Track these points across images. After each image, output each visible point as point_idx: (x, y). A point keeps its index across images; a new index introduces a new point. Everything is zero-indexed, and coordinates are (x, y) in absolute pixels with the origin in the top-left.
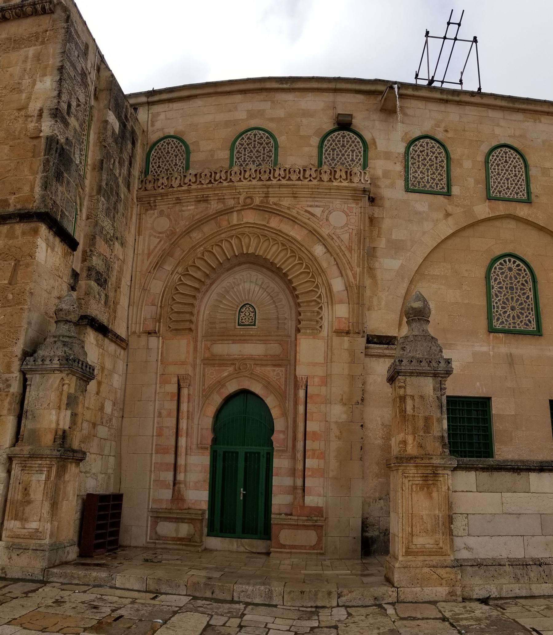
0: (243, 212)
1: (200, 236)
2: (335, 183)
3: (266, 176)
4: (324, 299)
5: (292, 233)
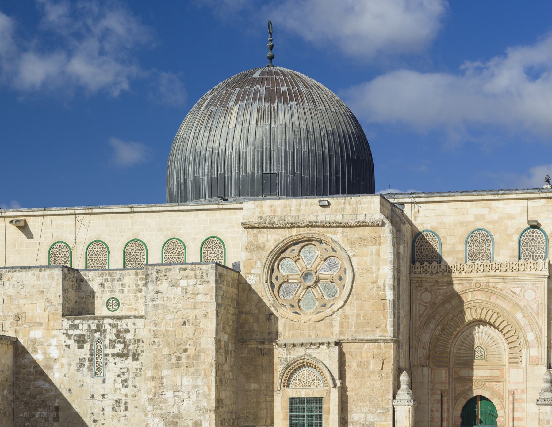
0: (474, 292)
1: (450, 306)
2: (527, 272)
3: (487, 269)
4: (523, 345)
5: (504, 306)
